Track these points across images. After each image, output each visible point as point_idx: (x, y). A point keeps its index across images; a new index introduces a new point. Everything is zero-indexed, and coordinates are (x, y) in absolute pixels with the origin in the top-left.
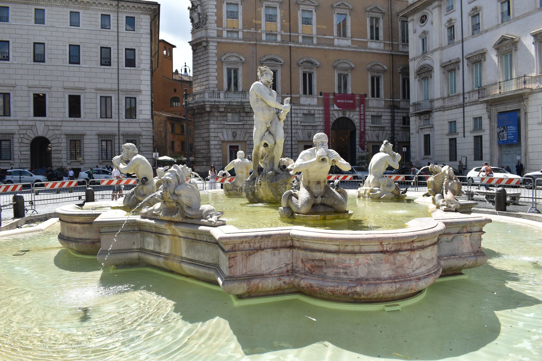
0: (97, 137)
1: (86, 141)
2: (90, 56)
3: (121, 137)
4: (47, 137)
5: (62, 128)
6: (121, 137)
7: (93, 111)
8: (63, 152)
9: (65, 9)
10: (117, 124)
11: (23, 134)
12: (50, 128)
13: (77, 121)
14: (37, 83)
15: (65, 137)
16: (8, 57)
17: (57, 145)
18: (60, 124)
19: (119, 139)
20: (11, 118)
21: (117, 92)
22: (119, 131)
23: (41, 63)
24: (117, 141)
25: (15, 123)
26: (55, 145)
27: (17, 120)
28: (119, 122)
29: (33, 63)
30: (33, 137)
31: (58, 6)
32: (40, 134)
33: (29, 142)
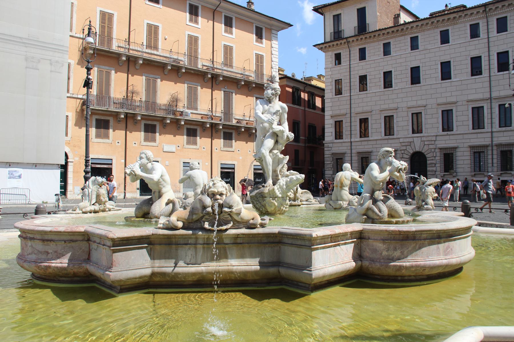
0: (469, 149)
1: (458, 154)
2: (461, 69)
3: (495, 148)
4: (423, 151)
5: (437, 142)
6: (495, 148)
7: (465, 123)
8: (437, 165)
9: (436, 30)
10: (490, 134)
11: (404, 150)
12: (426, 143)
13: (450, 135)
14: (414, 103)
15: (439, 150)
16: (391, 84)
17: (431, 158)
18: (434, 138)
19: (492, 150)
20: (395, 137)
21: (489, 101)
22: (492, 141)
23: (417, 85)
24: (490, 152)
25: (397, 141)
26: (430, 159)
27: (399, 138)
28: (492, 132)
29: (410, 86)
30: (411, 152)
31: (429, 29)
32: (417, 149)
33: (408, 157)
